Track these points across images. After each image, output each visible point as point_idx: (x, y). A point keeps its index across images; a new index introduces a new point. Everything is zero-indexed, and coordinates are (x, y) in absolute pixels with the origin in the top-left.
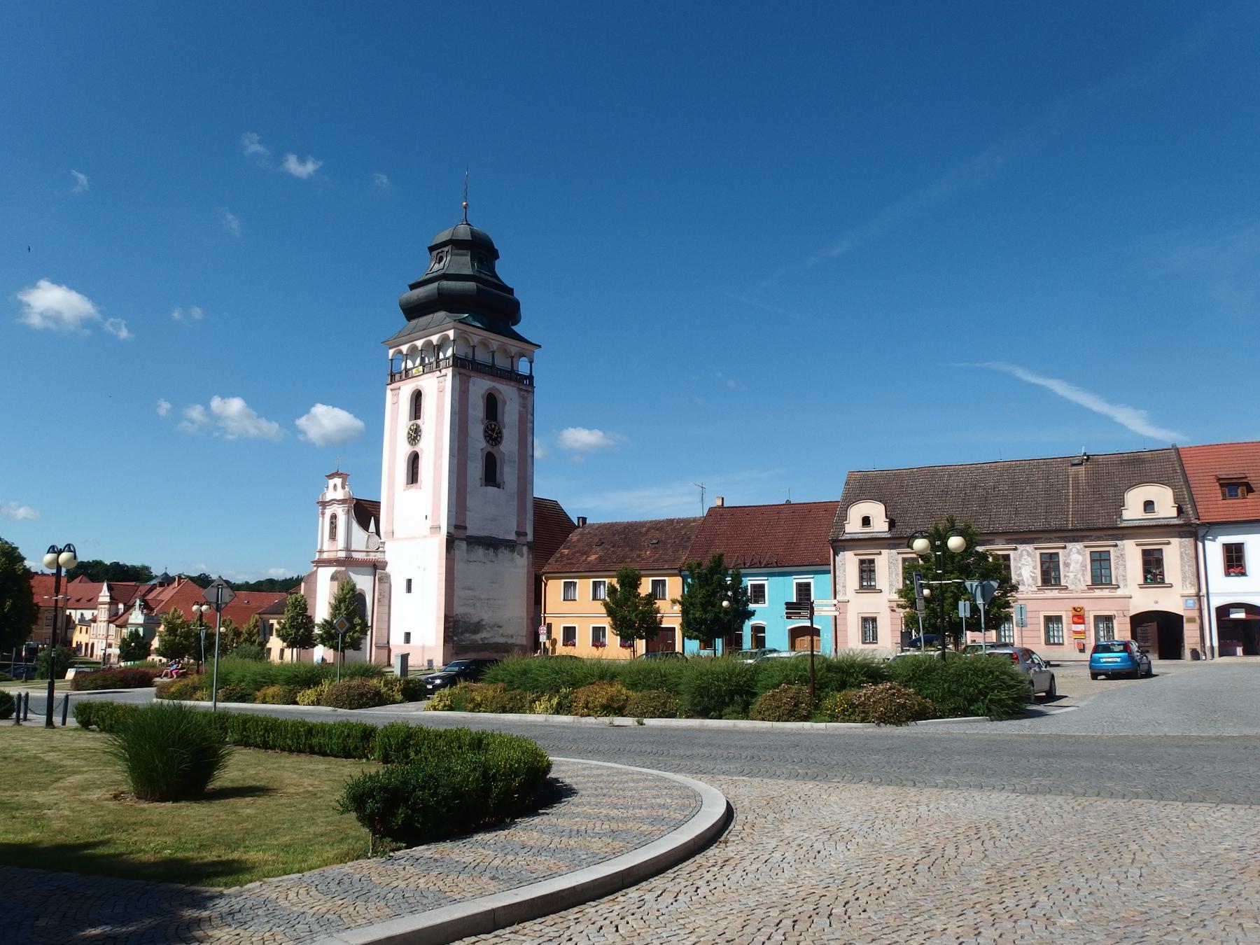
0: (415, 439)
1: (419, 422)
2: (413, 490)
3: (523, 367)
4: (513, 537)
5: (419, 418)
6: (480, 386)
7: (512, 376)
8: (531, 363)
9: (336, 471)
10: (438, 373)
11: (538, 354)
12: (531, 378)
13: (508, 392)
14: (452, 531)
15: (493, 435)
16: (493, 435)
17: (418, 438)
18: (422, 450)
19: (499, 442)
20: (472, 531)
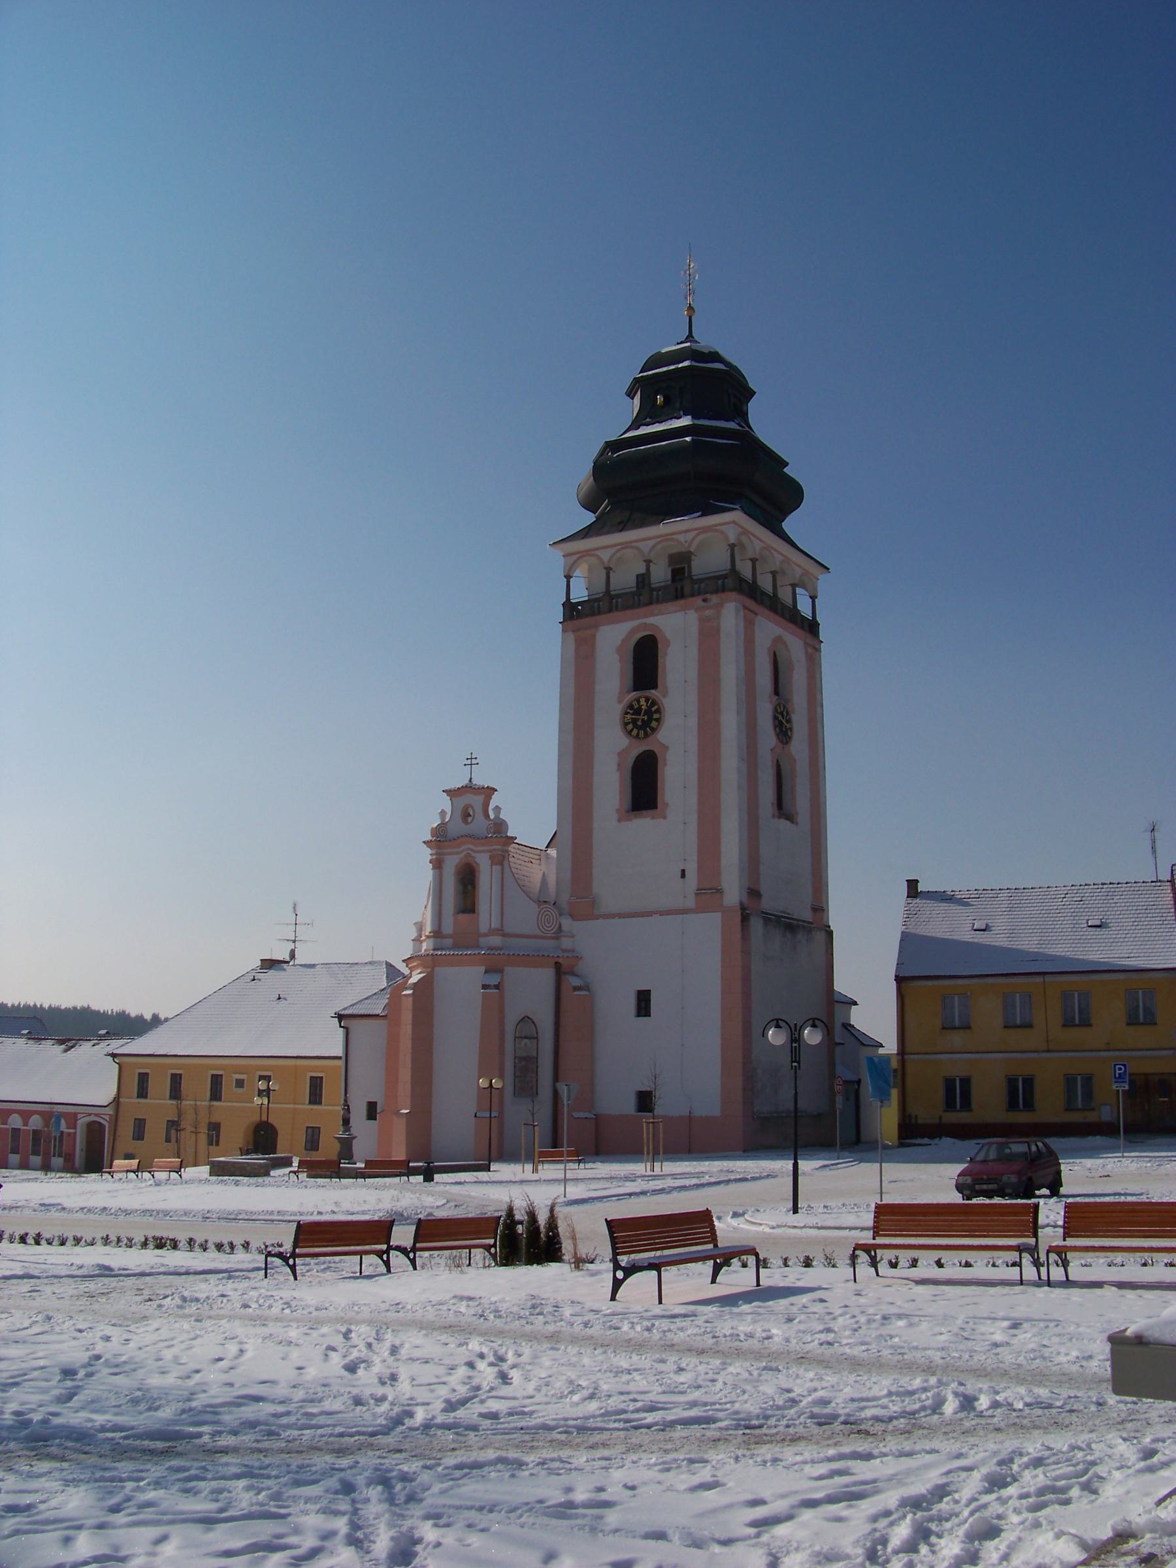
0: (646, 724)
1: (653, 693)
2: (643, 824)
3: (804, 607)
4: (807, 915)
5: (655, 687)
6: (768, 629)
7: (791, 616)
8: (813, 598)
9: (465, 782)
10: (698, 601)
11: (824, 583)
12: (811, 627)
13: (795, 643)
14: (745, 900)
15: (783, 728)
16: (783, 728)
17: (654, 724)
18: (665, 748)
19: (790, 738)
20: (767, 904)
